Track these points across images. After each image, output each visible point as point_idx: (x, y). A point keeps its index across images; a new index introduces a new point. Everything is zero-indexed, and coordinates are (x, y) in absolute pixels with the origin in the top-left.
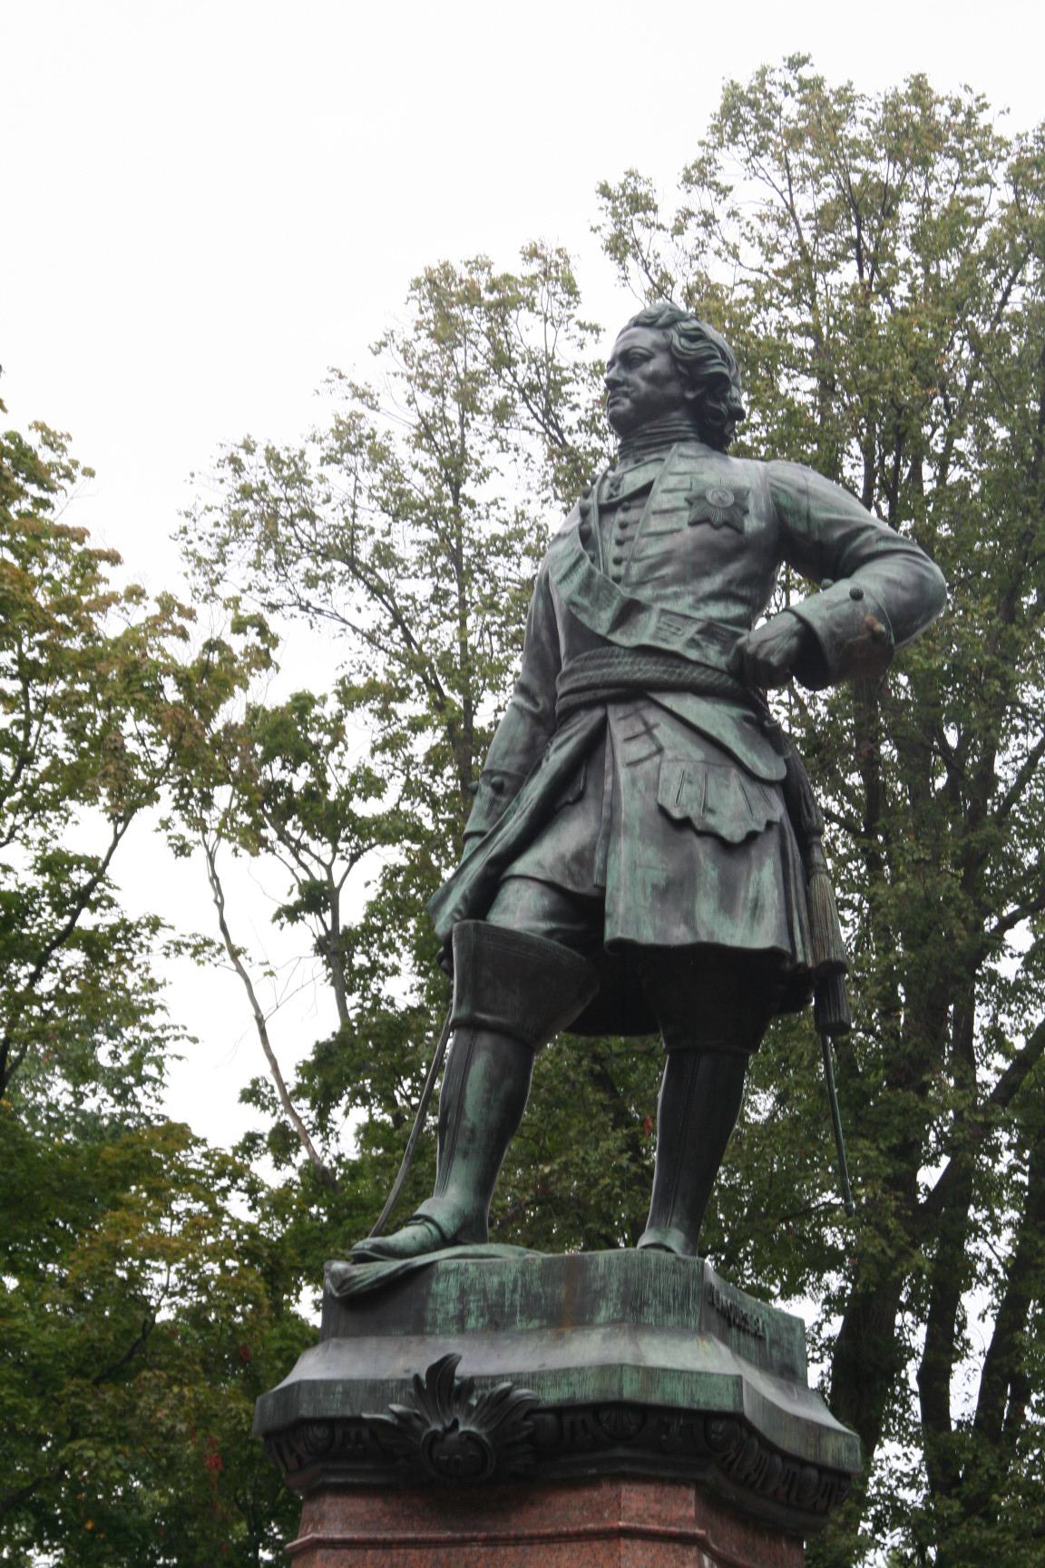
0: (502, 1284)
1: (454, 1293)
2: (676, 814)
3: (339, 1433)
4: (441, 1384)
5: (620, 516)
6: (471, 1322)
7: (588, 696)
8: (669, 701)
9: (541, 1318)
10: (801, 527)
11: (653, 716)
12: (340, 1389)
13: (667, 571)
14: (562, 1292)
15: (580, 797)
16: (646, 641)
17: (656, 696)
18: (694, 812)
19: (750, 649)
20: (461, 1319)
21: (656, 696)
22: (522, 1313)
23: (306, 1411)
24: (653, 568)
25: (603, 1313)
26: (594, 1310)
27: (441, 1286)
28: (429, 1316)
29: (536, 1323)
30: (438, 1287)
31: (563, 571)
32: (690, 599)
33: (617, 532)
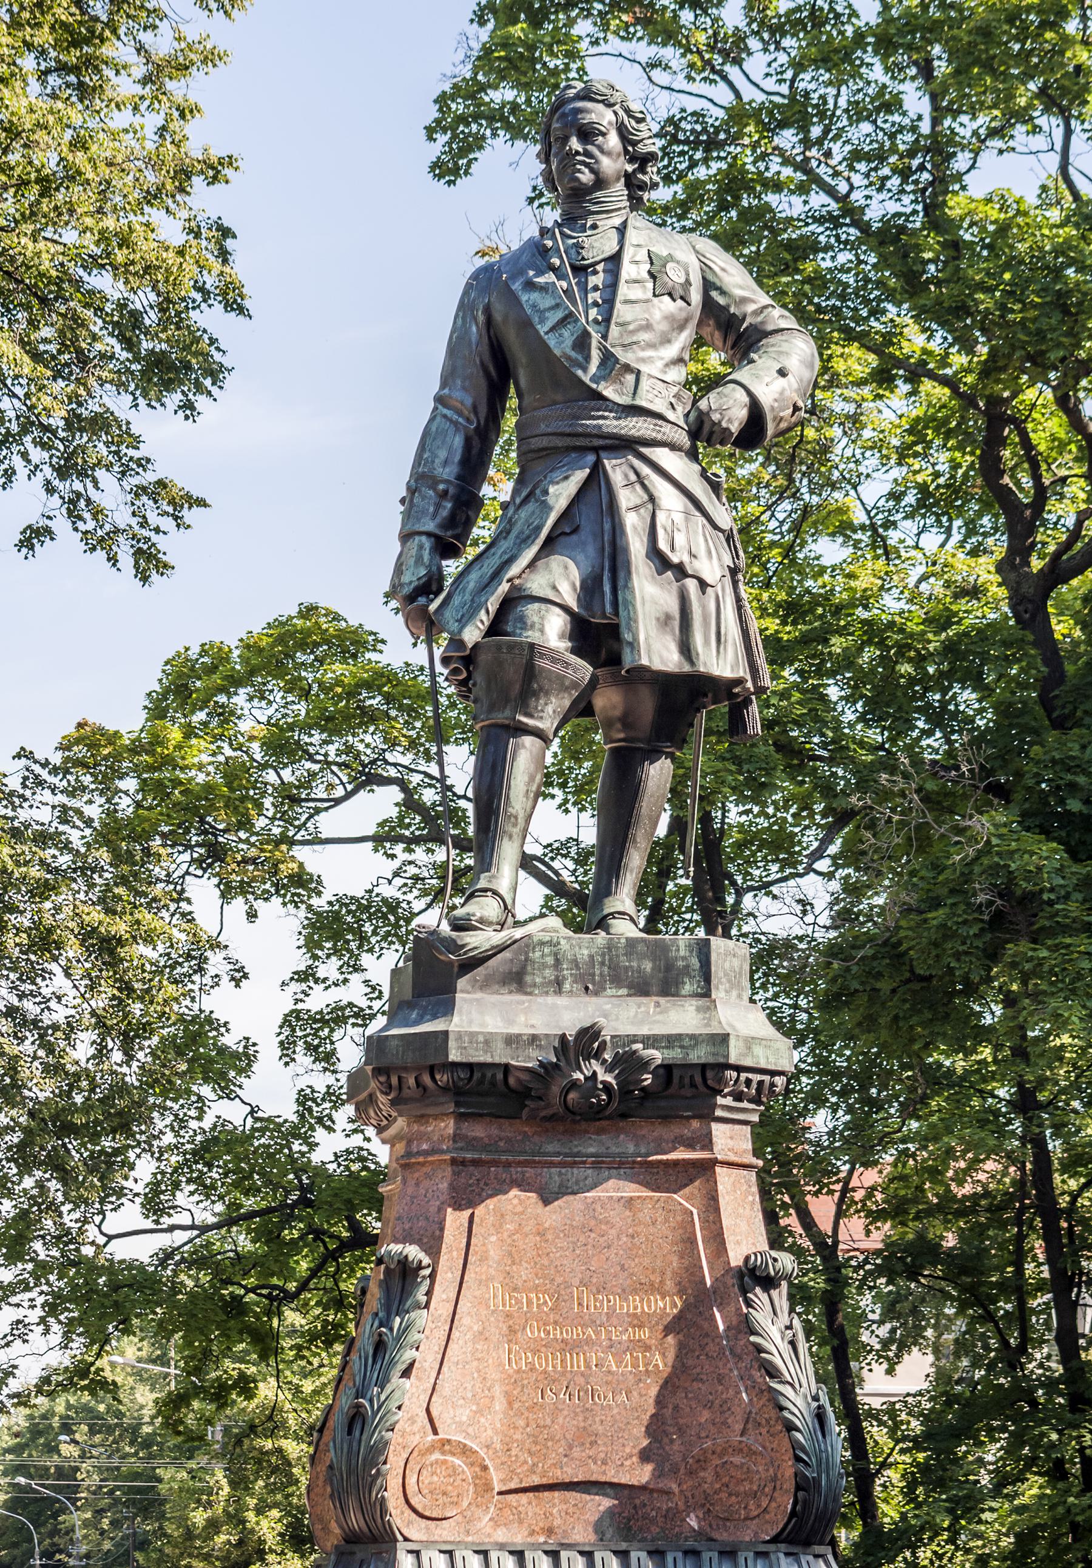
0: (591, 957)
1: (550, 960)
3: (477, 1075)
4: (587, 1042)
6: (567, 986)
9: (629, 987)
10: (721, 300)
11: (645, 470)
12: (481, 1039)
14: (648, 966)
15: (575, 531)
17: (645, 450)
18: (686, 559)
20: (558, 984)
21: (645, 450)
22: (612, 982)
23: (454, 1056)
25: (687, 987)
26: (679, 984)
27: (538, 954)
29: (624, 991)
31: (549, 324)
32: (660, 364)
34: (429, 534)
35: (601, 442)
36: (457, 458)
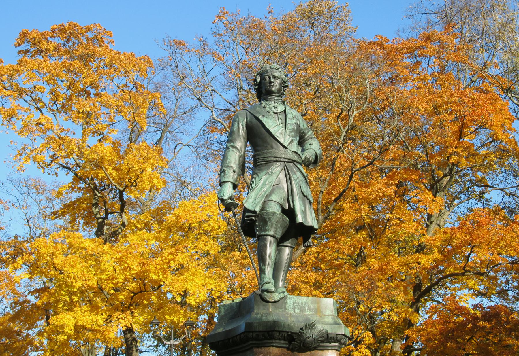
1: (292, 303)
2: (306, 194)
5: (280, 116)
7: (281, 160)
8: (299, 166)
13: (293, 134)
16: (295, 150)
19: (308, 157)
23: (276, 329)
24: (291, 132)
28: (287, 308)
30: (288, 301)
33: (280, 120)
34: (231, 182)
35: (286, 160)
36: (237, 162)
